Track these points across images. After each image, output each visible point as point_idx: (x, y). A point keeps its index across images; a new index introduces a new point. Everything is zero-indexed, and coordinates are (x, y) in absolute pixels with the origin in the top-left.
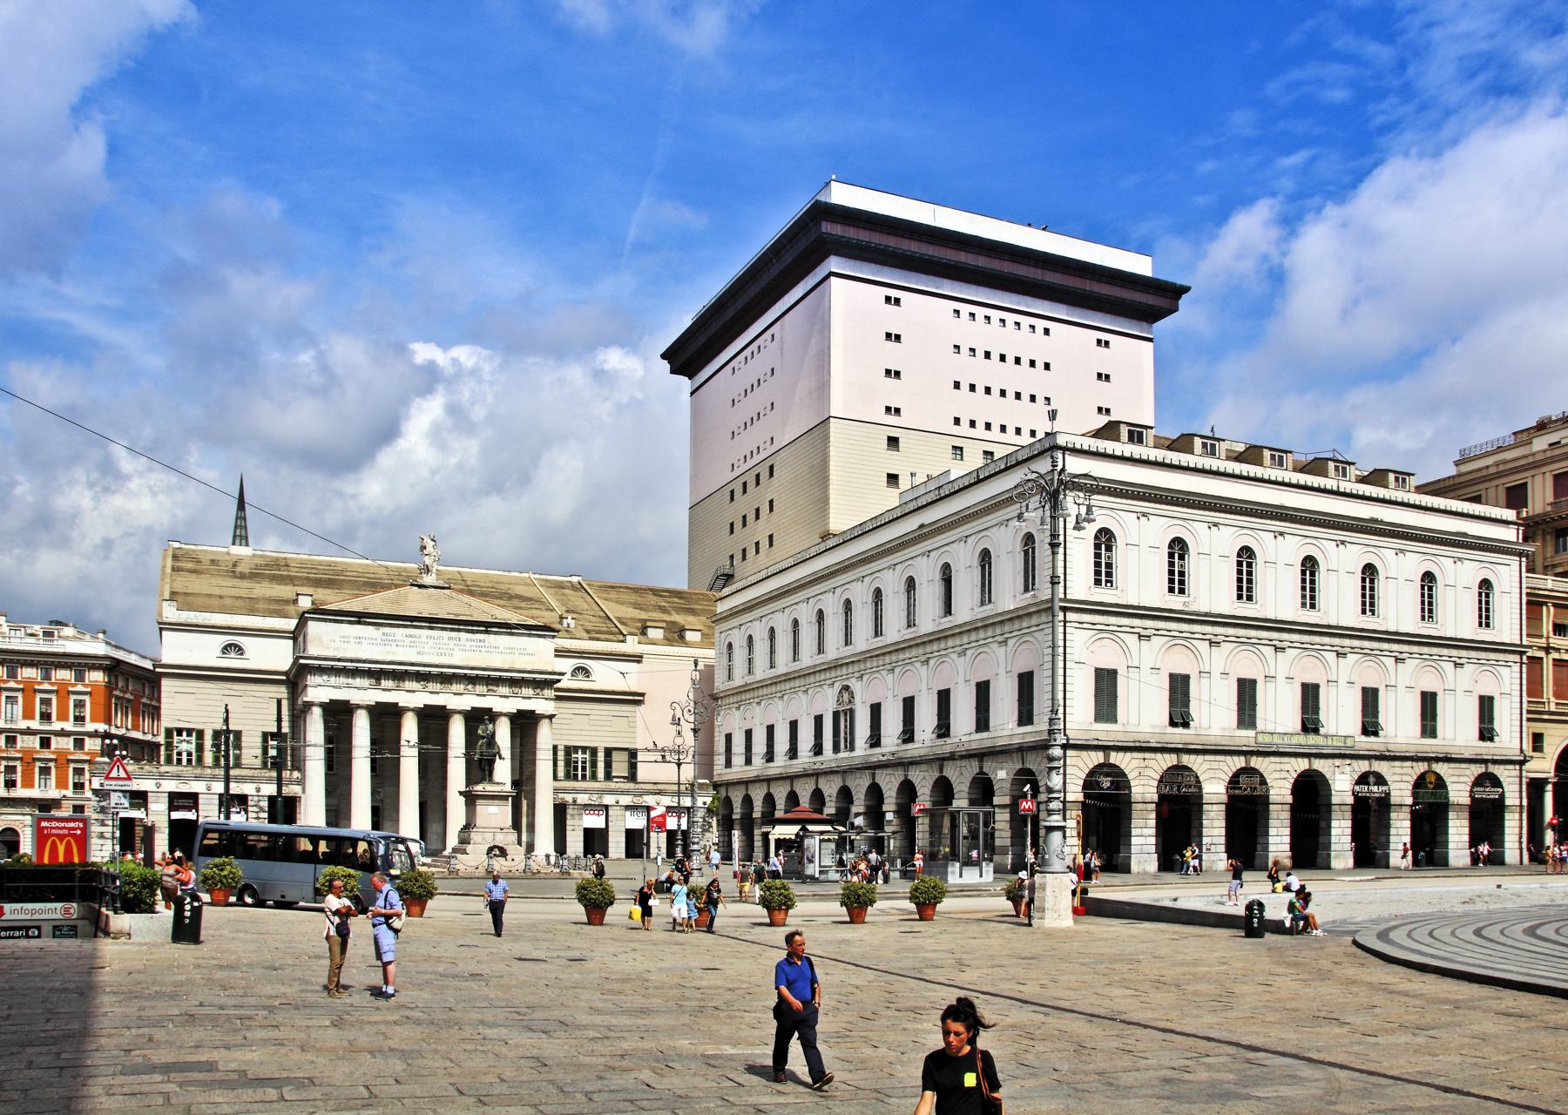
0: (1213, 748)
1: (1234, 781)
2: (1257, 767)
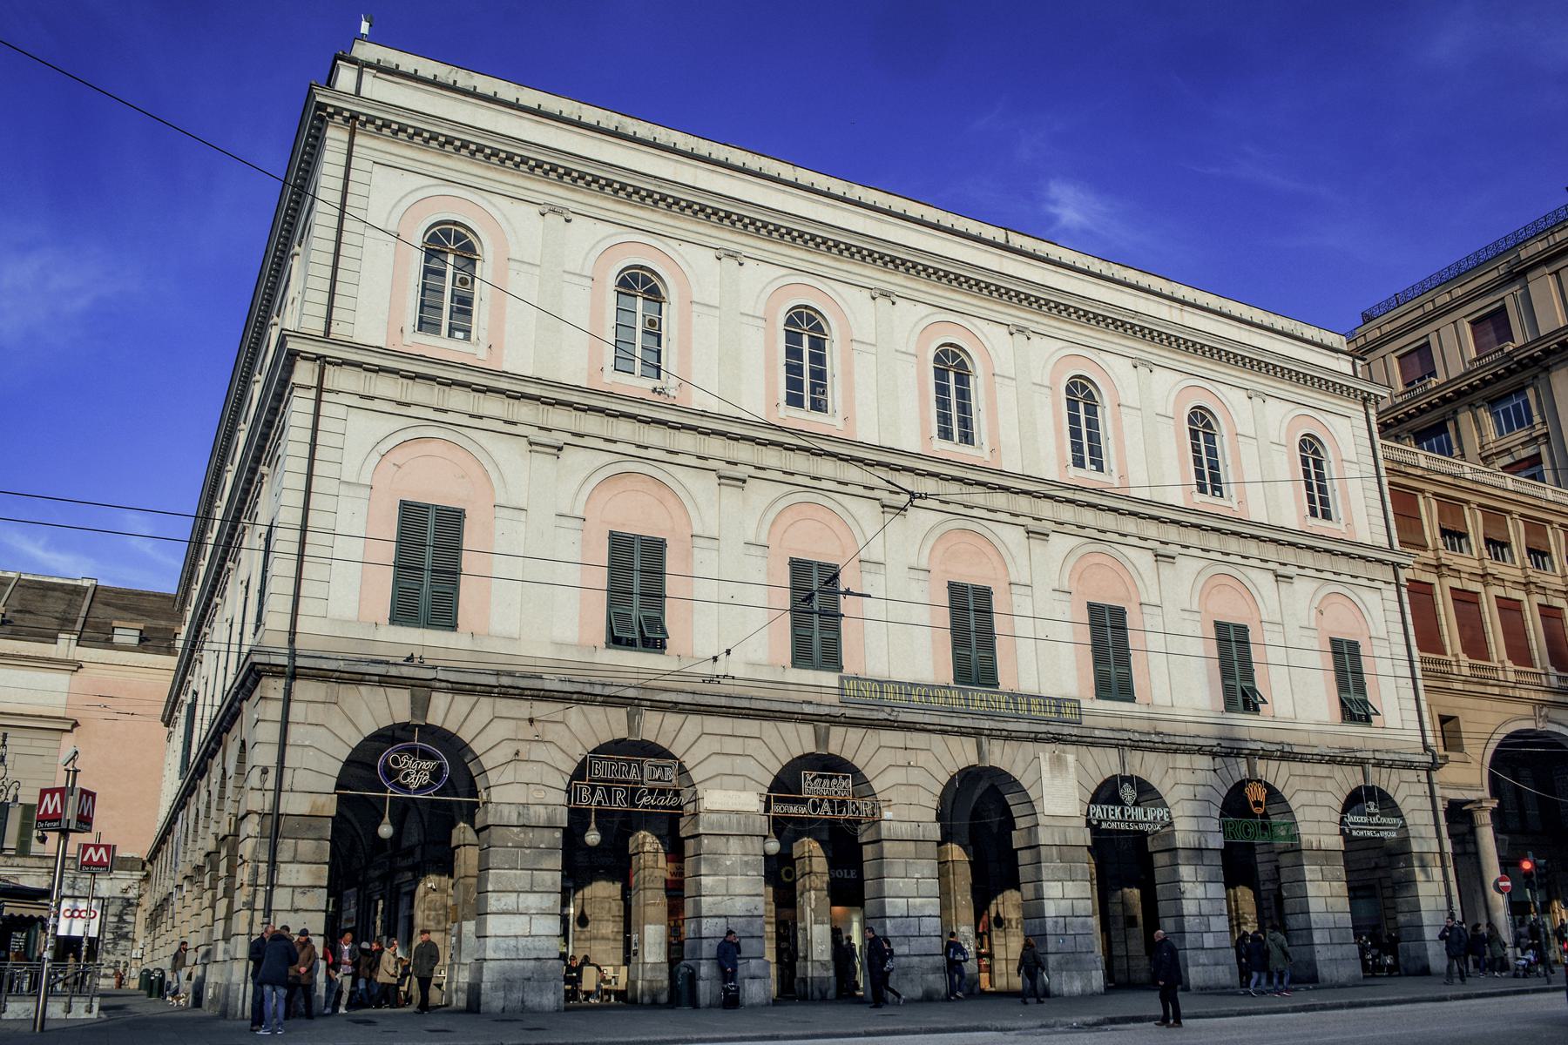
0: (723, 702)
1: (785, 785)
2: (847, 755)
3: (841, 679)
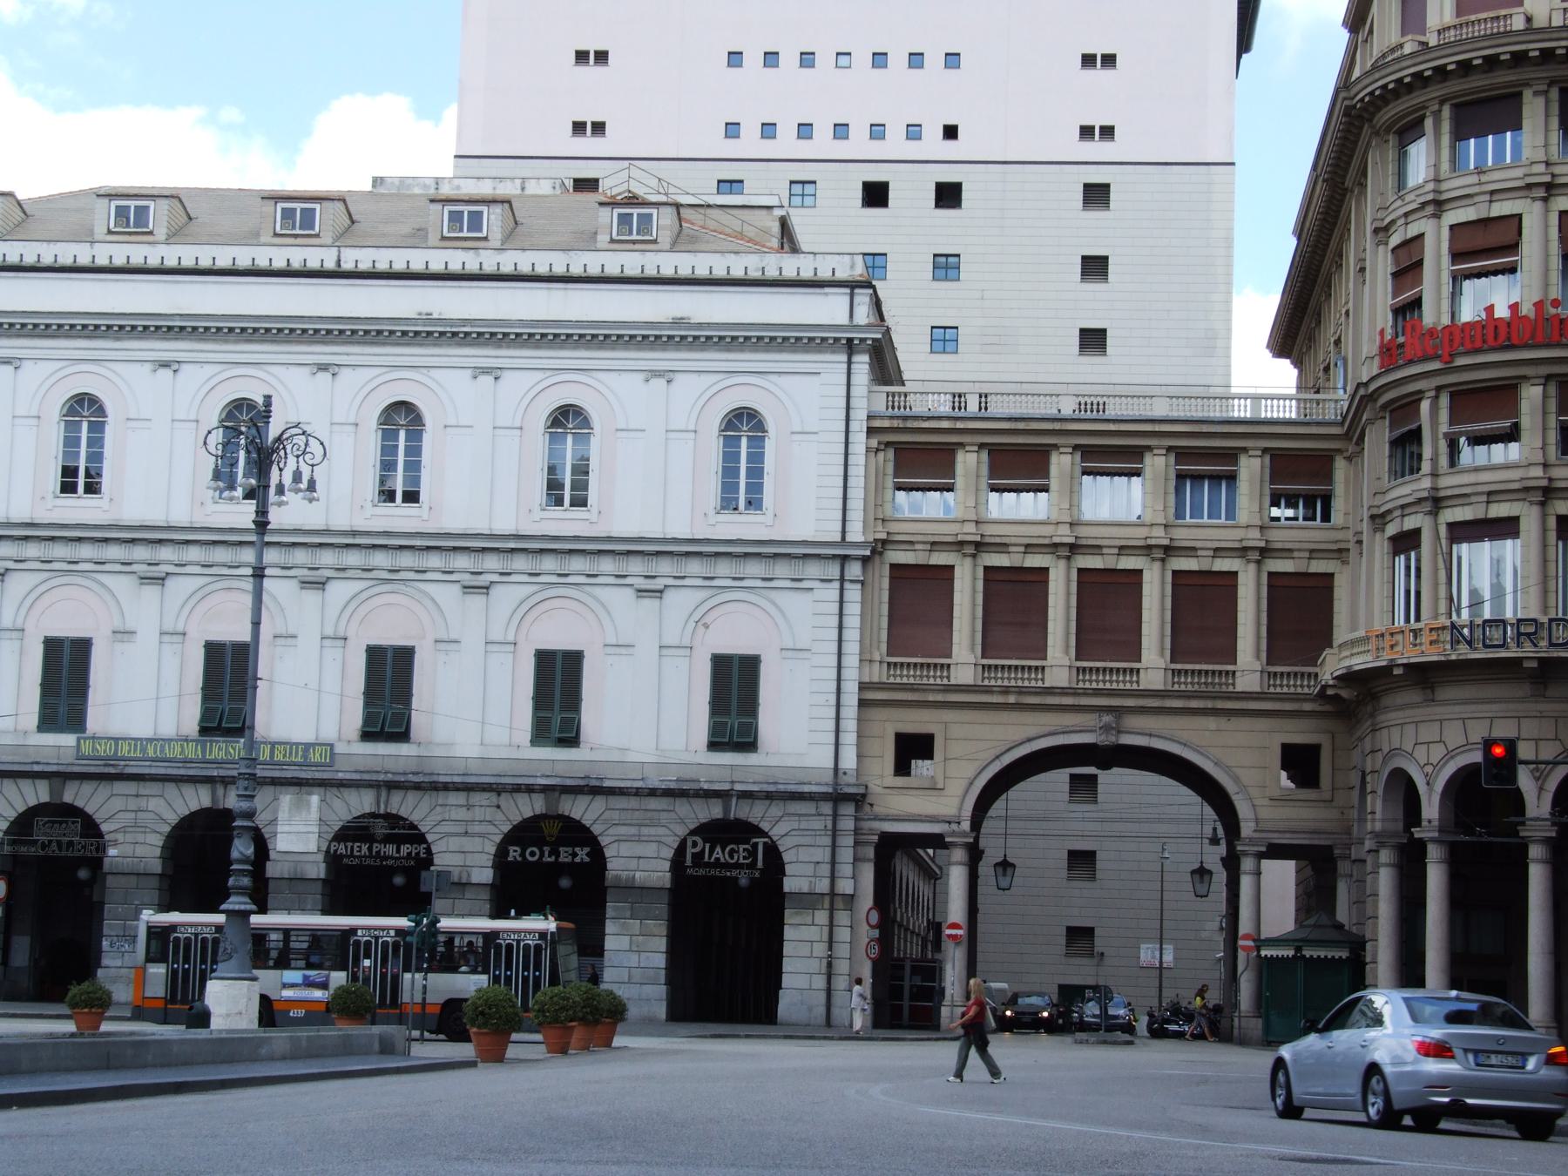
2: (79, 803)
3: (78, 740)
